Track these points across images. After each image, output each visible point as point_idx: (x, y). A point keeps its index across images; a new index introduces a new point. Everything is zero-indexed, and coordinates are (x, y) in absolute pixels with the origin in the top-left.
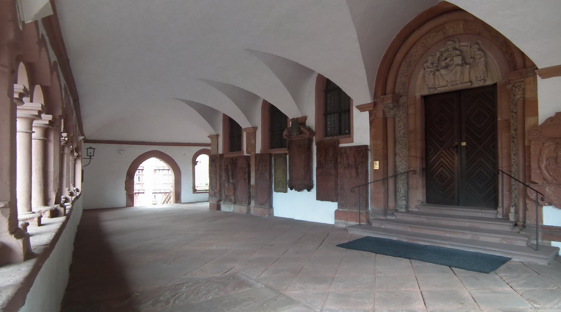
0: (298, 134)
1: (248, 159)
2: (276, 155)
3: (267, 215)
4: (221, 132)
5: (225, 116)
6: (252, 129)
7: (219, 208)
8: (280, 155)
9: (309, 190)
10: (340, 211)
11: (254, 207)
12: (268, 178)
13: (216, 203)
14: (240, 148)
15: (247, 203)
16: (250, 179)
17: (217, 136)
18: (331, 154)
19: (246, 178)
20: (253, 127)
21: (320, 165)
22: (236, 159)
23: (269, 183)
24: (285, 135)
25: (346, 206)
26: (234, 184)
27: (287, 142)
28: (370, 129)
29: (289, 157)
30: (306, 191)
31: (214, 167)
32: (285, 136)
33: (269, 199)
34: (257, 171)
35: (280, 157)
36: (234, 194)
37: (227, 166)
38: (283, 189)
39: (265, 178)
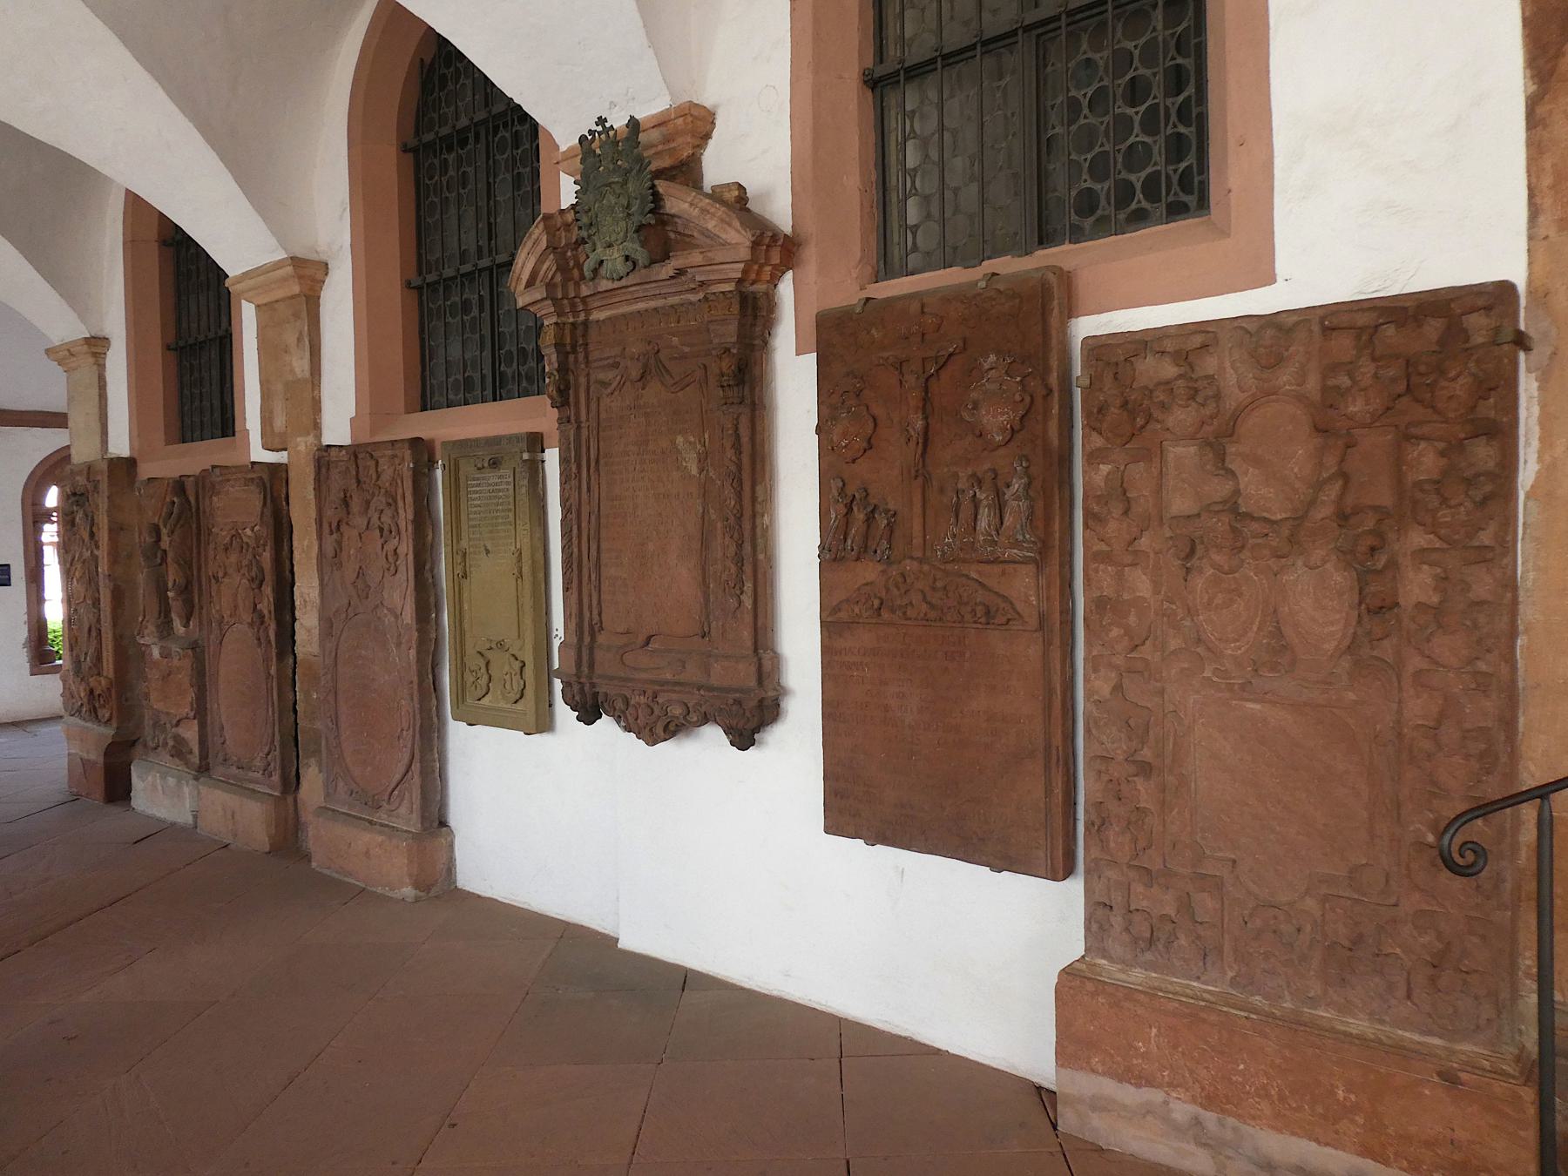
0: (641, 255)
1: (273, 480)
2: (464, 447)
3: (408, 891)
4: (115, 324)
5: (136, 205)
6: (290, 269)
7: (117, 788)
8: (492, 453)
9: (743, 738)
10: (1130, 993)
11: (322, 810)
12: (409, 615)
13: (101, 760)
14: (225, 424)
15: (276, 778)
16: (294, 620)
17: (97, 345)
18: (995, 420)
19: (266, 612)
20: (291, 258)
21: (870, 519)
22: (206, 482)
23: (413, 652)
24: (525, 277)
25: (1206, 954)
26: (195, 647)
27: (548, 339)
28: (1533, 106)
29: (564, 461)
30: (713, 736)
31: (86, 536)
32: (530, 283)
33: (416, 767)
34: (329, 562)
35: (495, 464)
36: (201, 711)
37: (156, 531)
38: (519, 706)
39: (389, 619)
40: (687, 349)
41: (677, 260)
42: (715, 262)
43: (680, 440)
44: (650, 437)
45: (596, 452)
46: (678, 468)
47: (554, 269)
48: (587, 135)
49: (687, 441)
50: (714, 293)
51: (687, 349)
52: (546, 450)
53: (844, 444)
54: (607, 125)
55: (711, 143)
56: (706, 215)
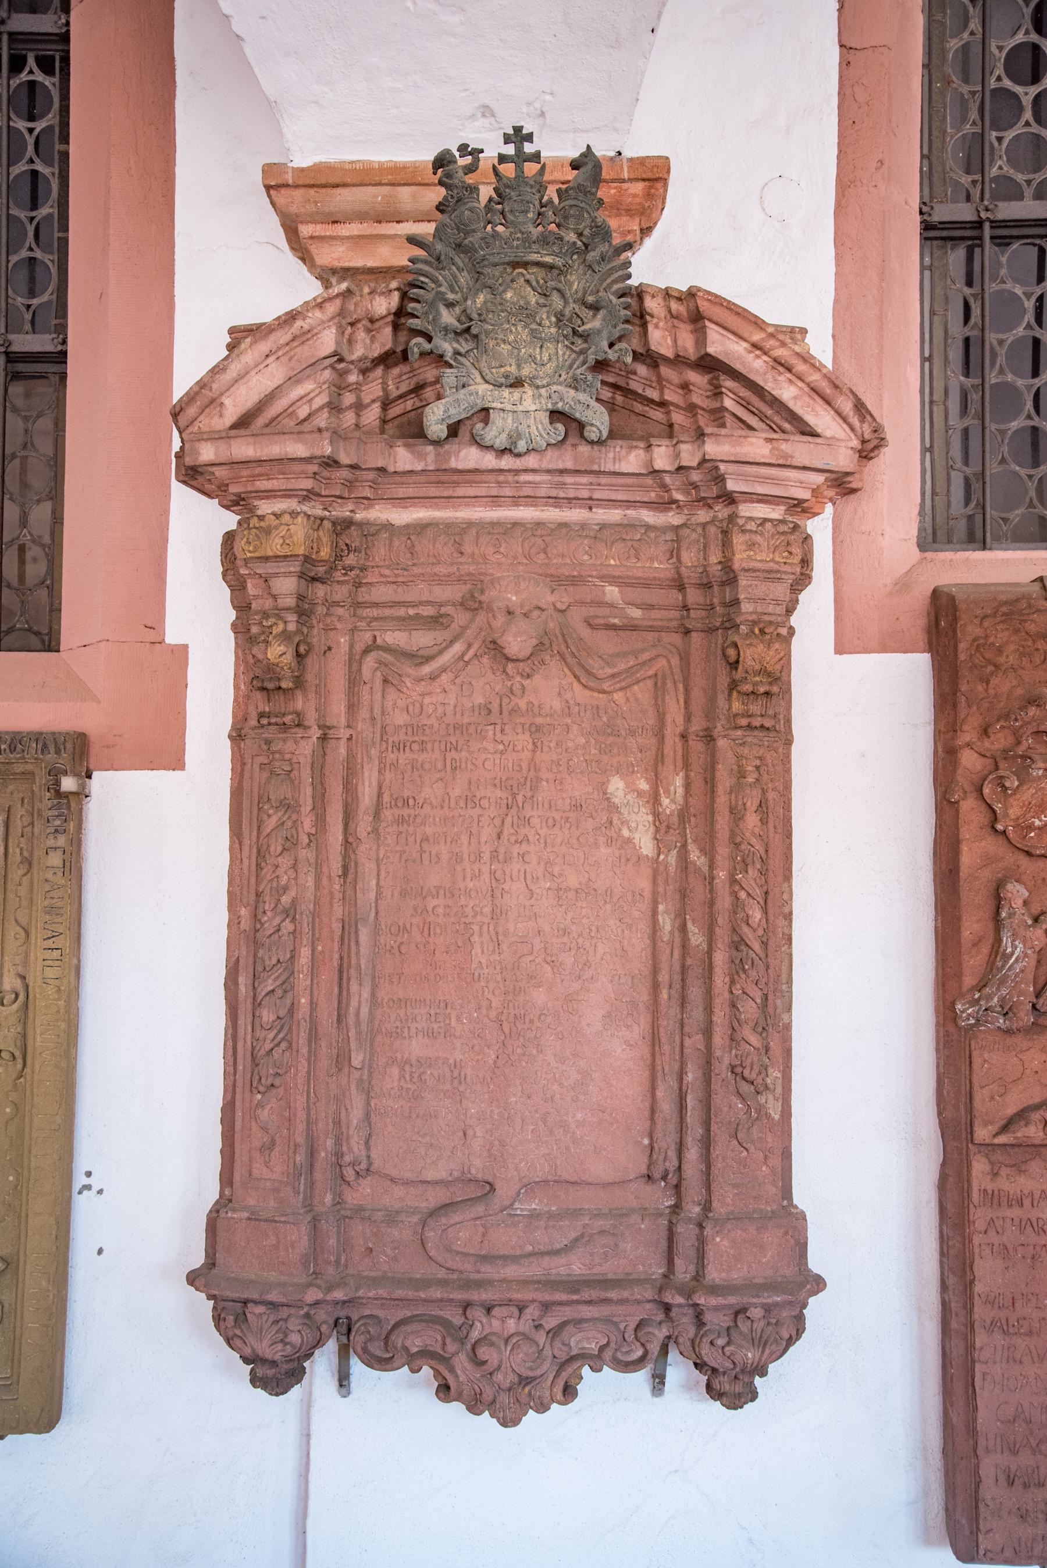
40: (636, 613)
41: (718, 444)
42: (794, 464)
43: (616, 786)
44: (544, 775)
45: (375, 793)
46: (610, 842)
47: (319, 402)
48: (457, 154)
49: (631, 788)
50: (751, 519)
51: (636, 613)
52: (96, 775)
53: (1037, 823)
54: (528, 148)
55: (649, 243)
56: (780, 374)
